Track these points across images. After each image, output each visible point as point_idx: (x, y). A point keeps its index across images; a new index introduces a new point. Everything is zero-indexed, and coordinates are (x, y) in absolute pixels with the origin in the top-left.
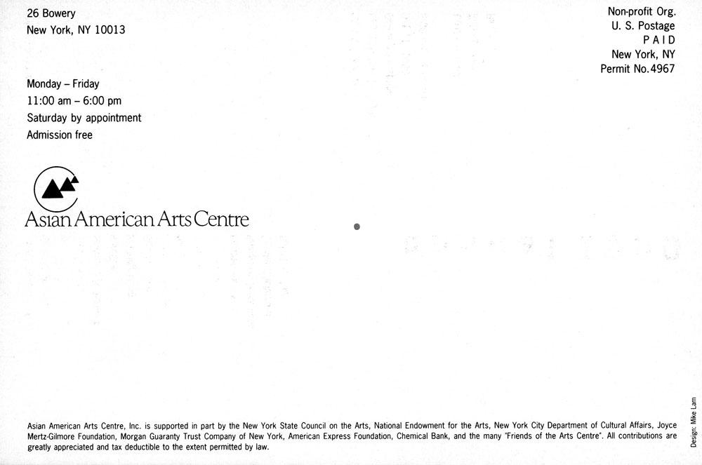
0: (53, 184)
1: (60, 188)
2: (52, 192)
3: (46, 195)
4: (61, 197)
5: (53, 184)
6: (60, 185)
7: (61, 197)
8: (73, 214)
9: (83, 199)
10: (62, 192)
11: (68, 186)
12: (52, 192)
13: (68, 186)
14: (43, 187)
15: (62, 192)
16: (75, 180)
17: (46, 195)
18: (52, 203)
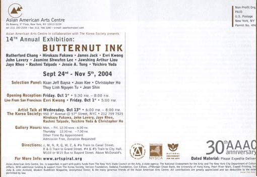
0: (14, 9)
1: (16, 9)
2: (14, 11)
3: (12, 13)
4: (17, 13)
5: (14, 9)
6: (16, 9)
7: (17, 13)
8: (19, 19)
9: (24, 14)
10: (17, 12)
11: (19, 9)
12: (14, 11)
13: (19, 9)
14: (11, 10)
15: (17, 12)
16: (21, 8)
17: (12, 13)
18: (14, 15)
